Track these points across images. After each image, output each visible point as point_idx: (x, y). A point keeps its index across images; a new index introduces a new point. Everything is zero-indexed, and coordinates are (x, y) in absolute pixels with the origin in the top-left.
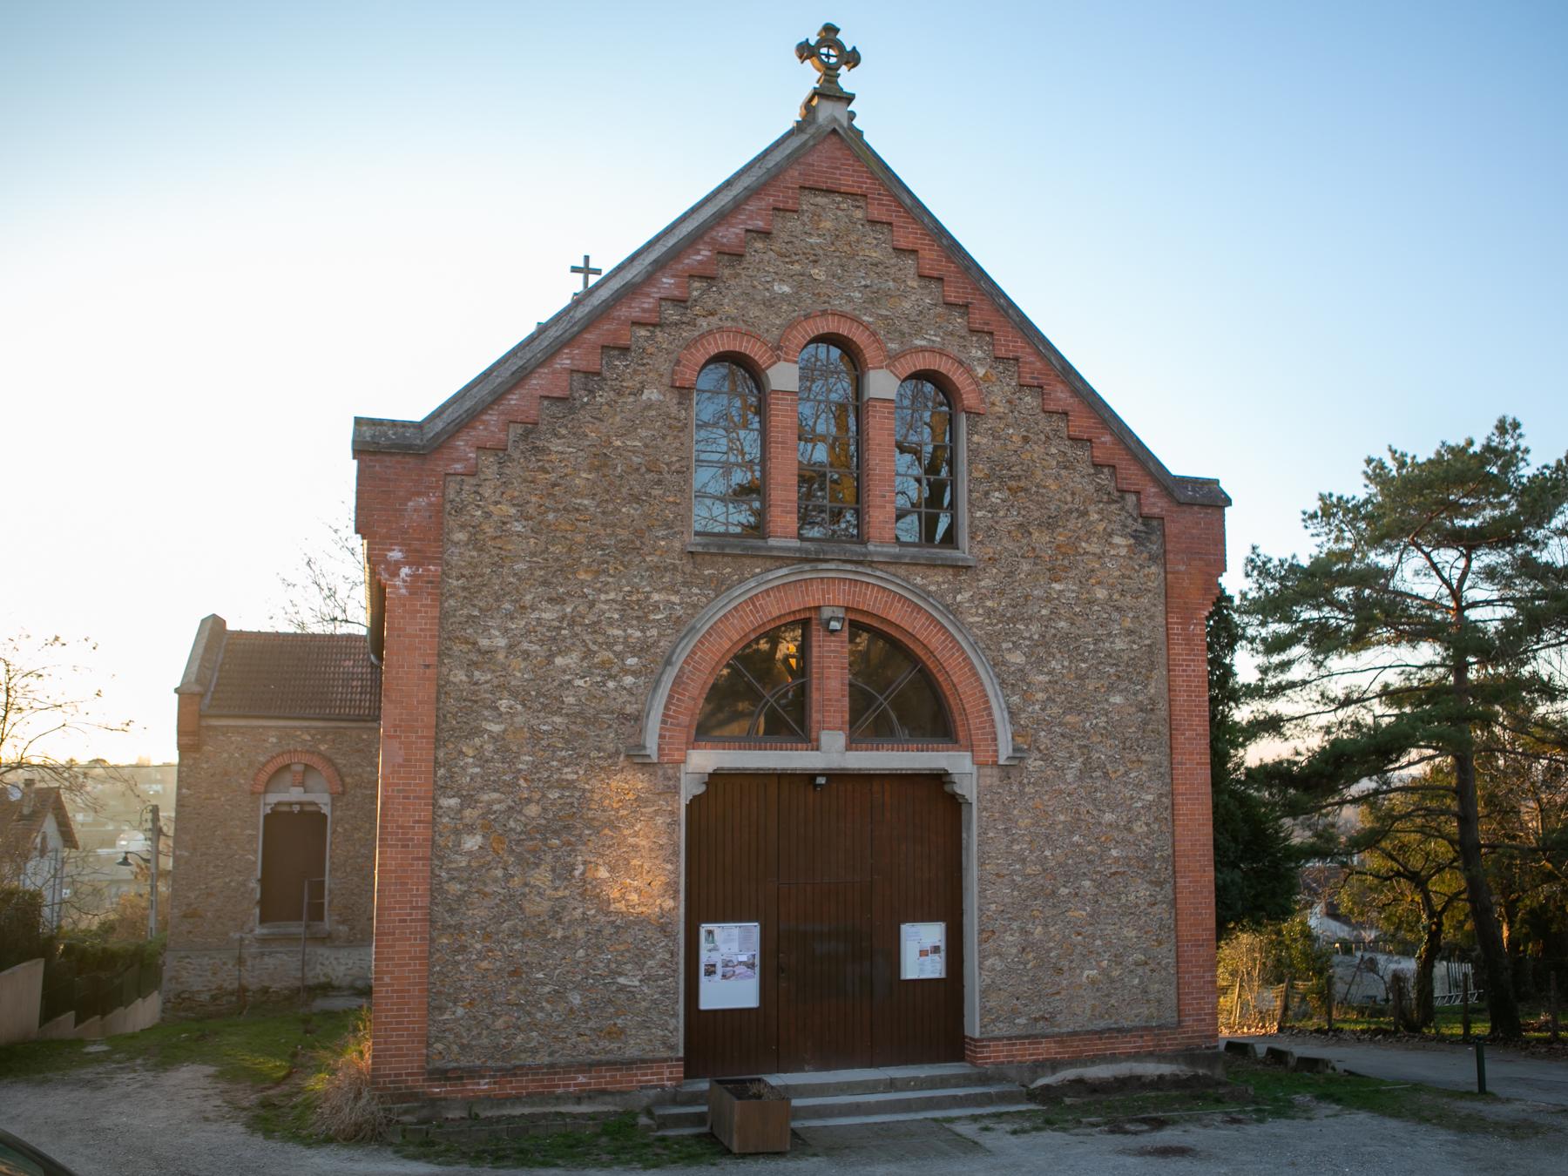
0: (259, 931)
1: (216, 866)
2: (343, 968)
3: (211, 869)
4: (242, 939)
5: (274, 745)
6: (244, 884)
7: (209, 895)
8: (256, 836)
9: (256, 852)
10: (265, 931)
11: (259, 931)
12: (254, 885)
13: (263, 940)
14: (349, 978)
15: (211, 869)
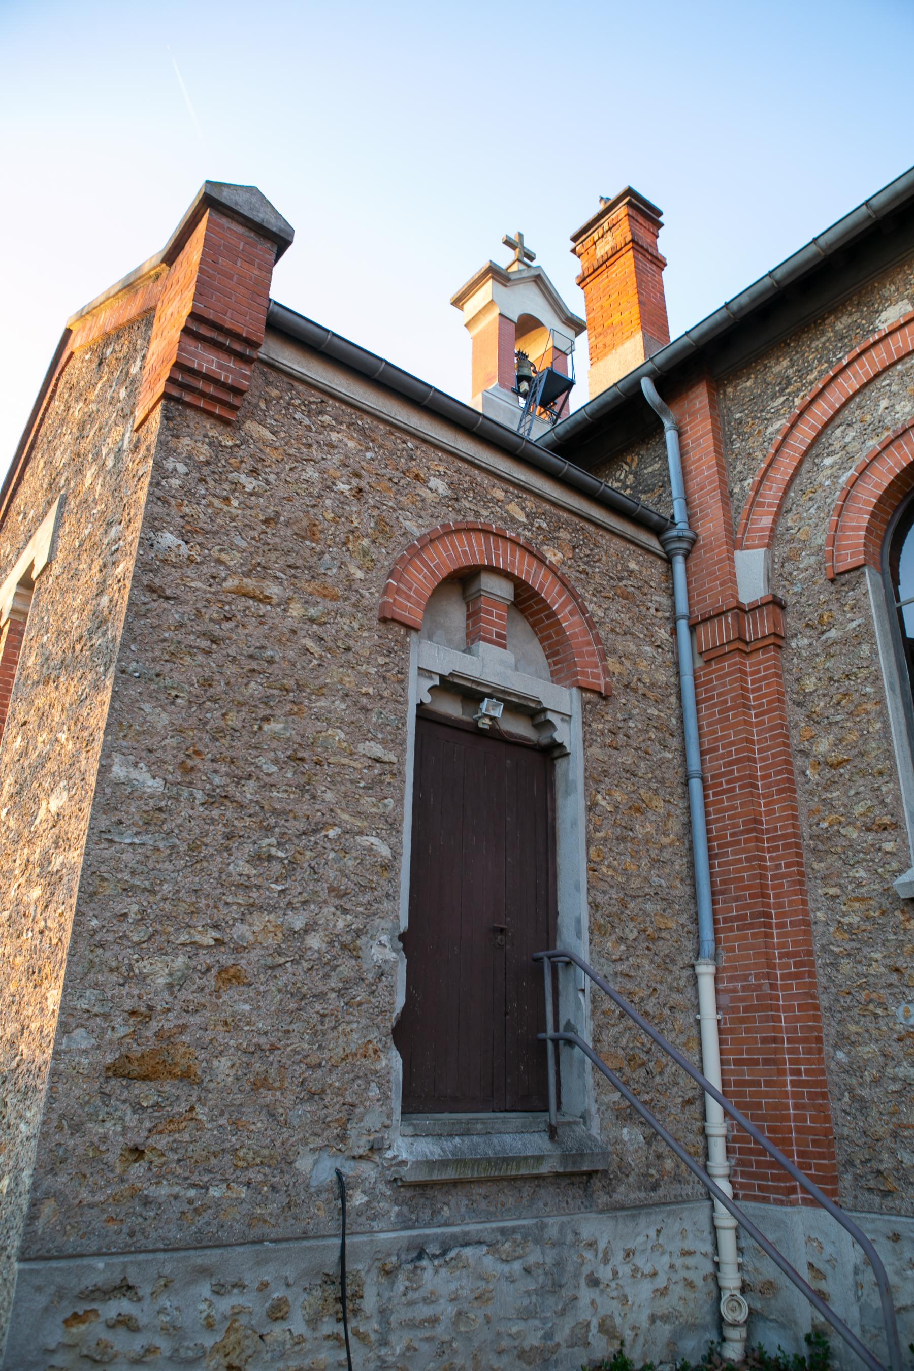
0: (409, 1148)
1: (260, 858)
2: (646, 1289)
3: (241, 867)
4: (342, 1187)
5: (445, 501)
6: (351, 950)
7: (230, 977)
8: (398, 774)
9: (393, 826)
10: (428, 1148)
11: (409, 1148)
12: (384, 952)
13: (420, 1191)
14: (665, 1331)
15: (241, 867)
